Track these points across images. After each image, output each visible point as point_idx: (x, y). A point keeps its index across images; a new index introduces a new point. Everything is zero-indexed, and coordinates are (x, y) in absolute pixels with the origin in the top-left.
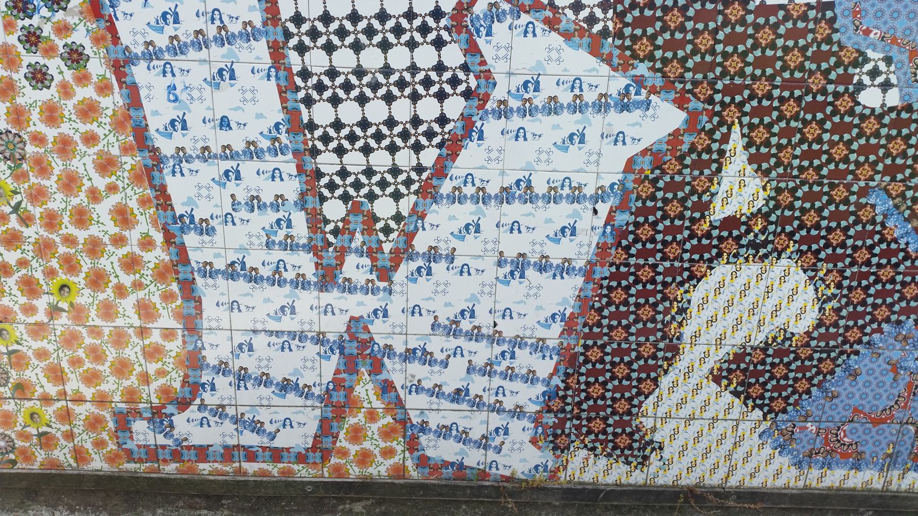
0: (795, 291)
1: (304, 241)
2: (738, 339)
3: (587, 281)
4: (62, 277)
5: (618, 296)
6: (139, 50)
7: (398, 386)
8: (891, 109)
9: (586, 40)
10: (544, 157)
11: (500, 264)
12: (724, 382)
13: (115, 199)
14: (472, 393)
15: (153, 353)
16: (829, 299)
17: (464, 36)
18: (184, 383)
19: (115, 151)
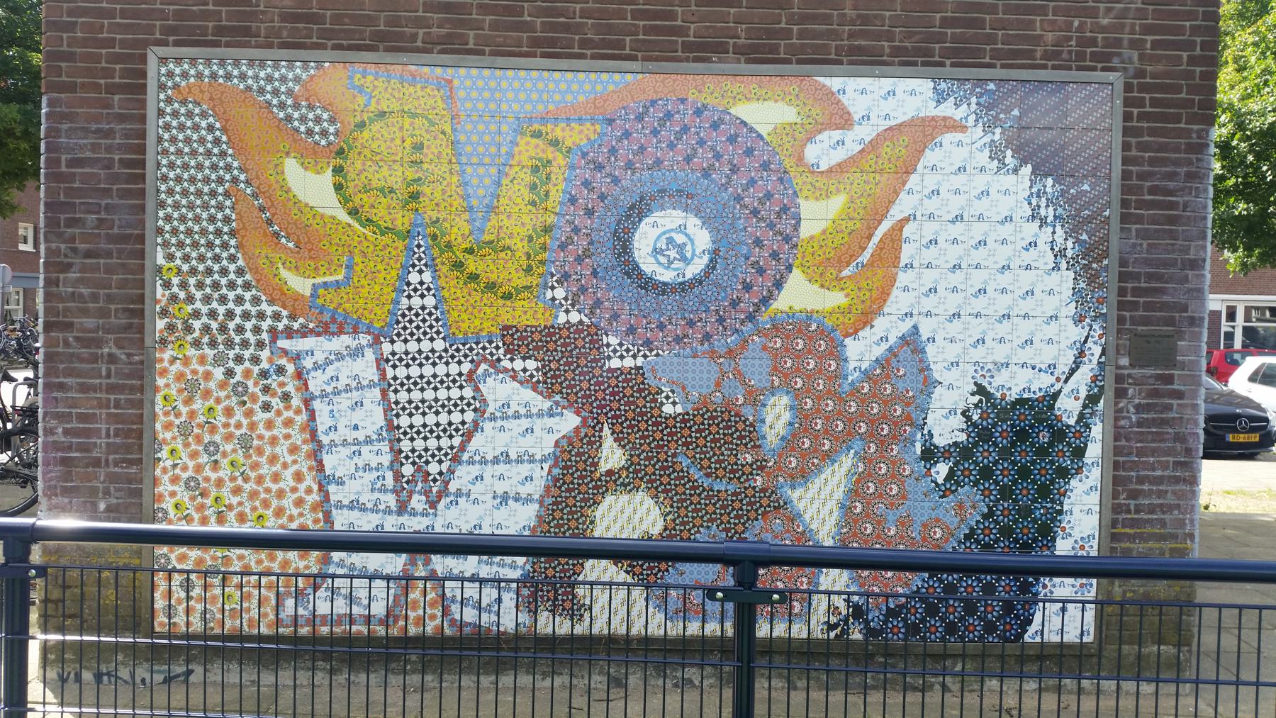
3: (540, 507)
4: (260, 511)
5: (558, 514)
6: (317, 394)
8: (679, 414)
9: (530, 385)
10: (514, 440)
13: (296, 467)
19: (299, 443)
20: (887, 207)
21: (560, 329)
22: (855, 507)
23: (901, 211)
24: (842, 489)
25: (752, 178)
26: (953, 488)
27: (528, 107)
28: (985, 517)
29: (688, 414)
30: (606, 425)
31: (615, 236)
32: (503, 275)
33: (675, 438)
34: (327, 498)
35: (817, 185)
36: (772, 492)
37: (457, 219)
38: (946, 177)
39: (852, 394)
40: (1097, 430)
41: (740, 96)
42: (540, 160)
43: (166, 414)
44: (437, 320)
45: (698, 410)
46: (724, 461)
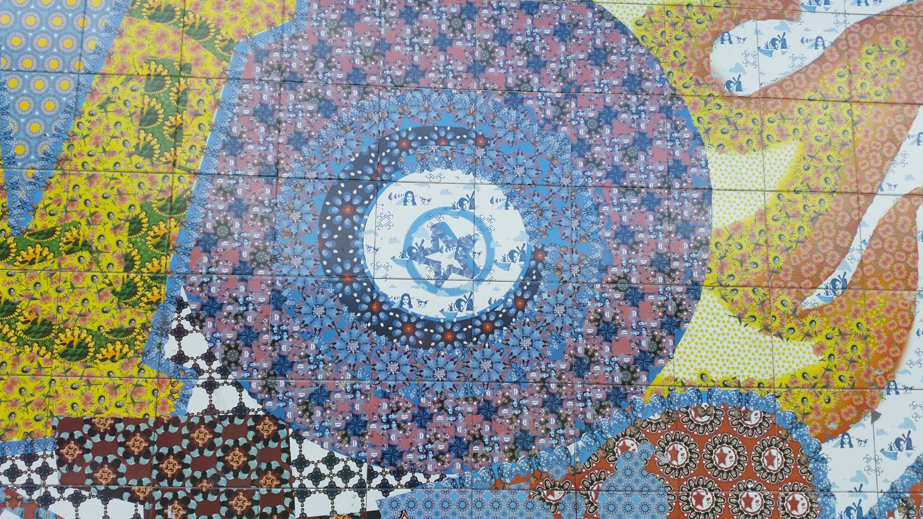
20: (880, 169)
21: (192, 427)
23: (909, 178)
25: (608, 108)
31: (322, 220)
32: (72, 304)
35: (740, 122)
42: (167, 63)
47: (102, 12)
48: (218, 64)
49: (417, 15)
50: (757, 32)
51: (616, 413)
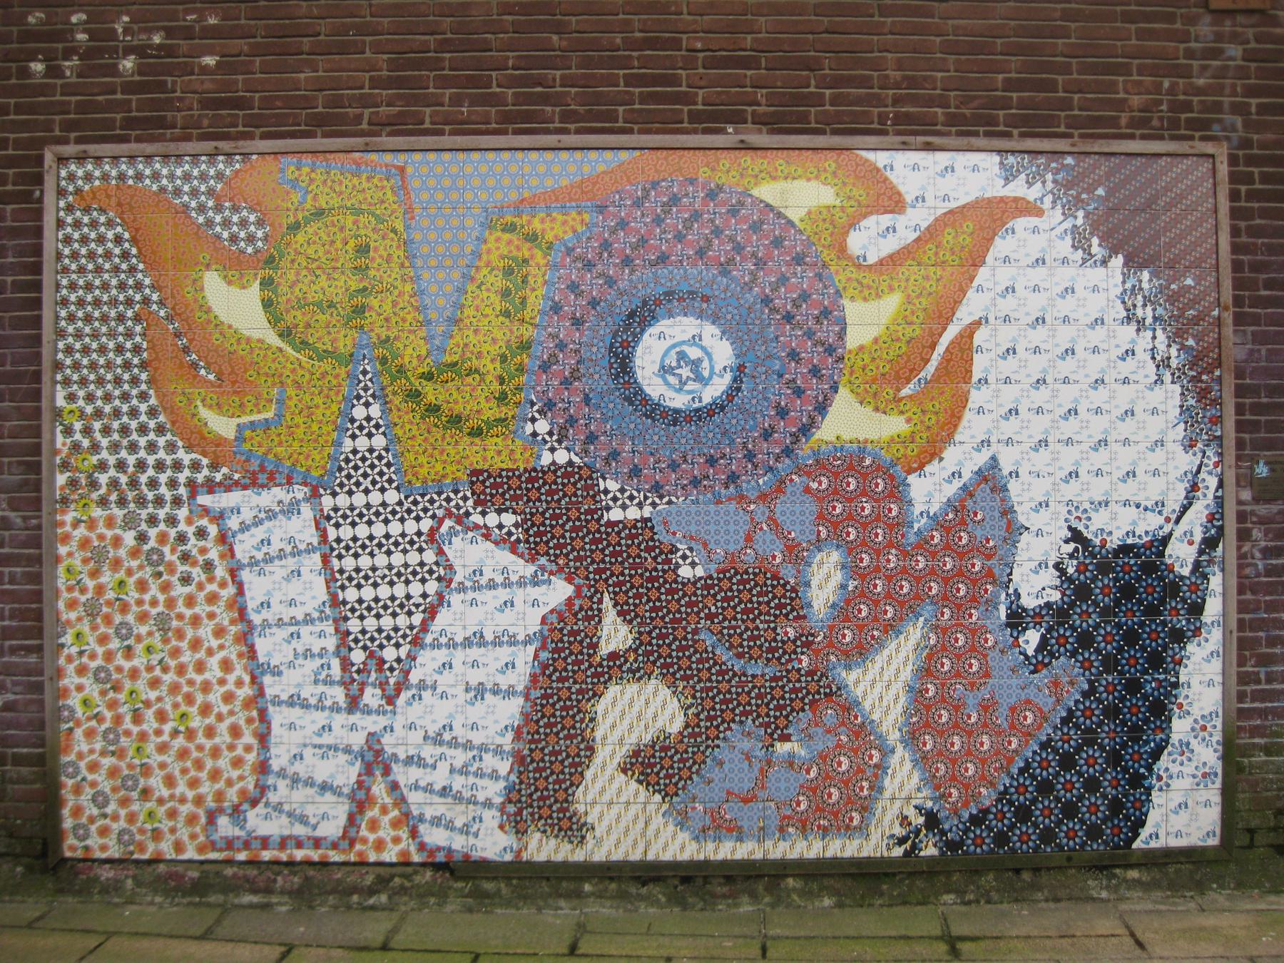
0: (665, 703)
1: (338, 678)
2: (633, 739)
4: (183, 708)
6: (246, 561)
7: (402, 784)
8: (700, 578)
9: (508, 545)
10: (489, 616)
11: (467, 690)
12: (630, 773)
13: (223, 654)
14: (455, 789)
15: (237, 763)
16: (689, 707)
17: (435, 545)
18: (256, 786)
19: (226, 623)
21: (544, 473)
22: (927, 690)
23: (970, 314)
24: (910, 667)
26: (1046, 661)
27: (499, 196)
28: (1086, 695)
29: (710, 577)
30: (606, 594)
31: (610, 351)
32: (472, 405)
33: (696, 609)
34: (261, 693)
35: (865, 281)
36: (822, 675)
37: (412, 337)
38: (1021, 271)
39: (918, 546)
40: (1216, 582)
41: (763, 175)
42: (514, 259)
43: (70, 589)
44: (389, 465)
45: (724, 571)
46: (759, 637)
47: (473, 229)
48: (544, 257)
49: (663, 220)
50: (878, 223)
51: (787, 461)
